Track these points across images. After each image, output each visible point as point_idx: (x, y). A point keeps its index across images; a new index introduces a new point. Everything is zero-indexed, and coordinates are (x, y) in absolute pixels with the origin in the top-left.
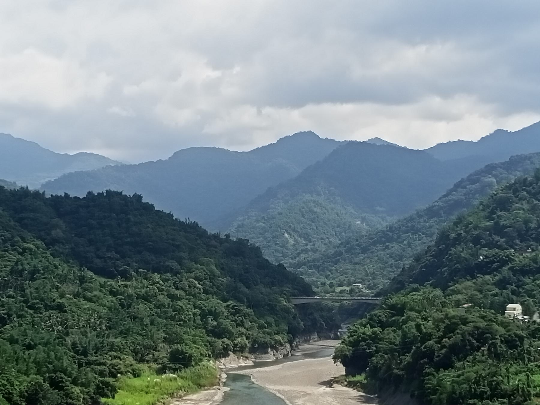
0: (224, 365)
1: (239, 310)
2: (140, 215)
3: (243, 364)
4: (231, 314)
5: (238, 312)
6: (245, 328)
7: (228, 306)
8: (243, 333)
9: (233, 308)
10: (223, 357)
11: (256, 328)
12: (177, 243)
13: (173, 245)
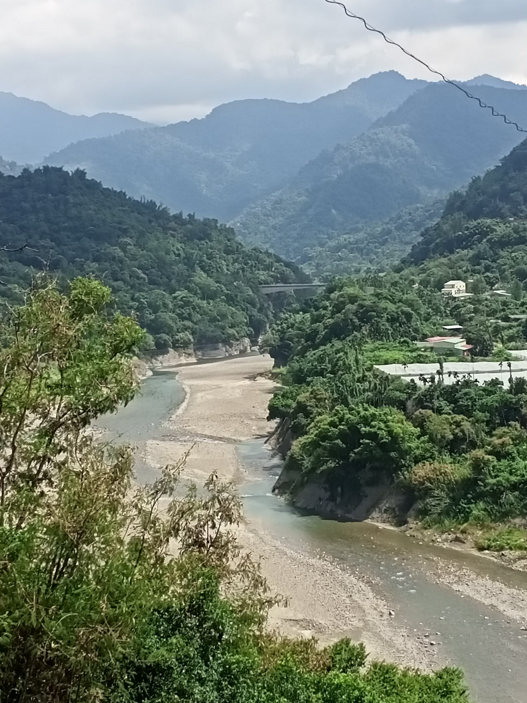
0: (161, 363)
1: (189, 301)
2: (82, 195)
3: (184, 362)
4: (179, 307)
5: (187, 303)
6: (192, 322)
7: (175, 298)
8: (189, 328)
9: (181, 299)
10: (161, 354)
11: (207, 321)
12: (124, 227)
13: (119, 229)
